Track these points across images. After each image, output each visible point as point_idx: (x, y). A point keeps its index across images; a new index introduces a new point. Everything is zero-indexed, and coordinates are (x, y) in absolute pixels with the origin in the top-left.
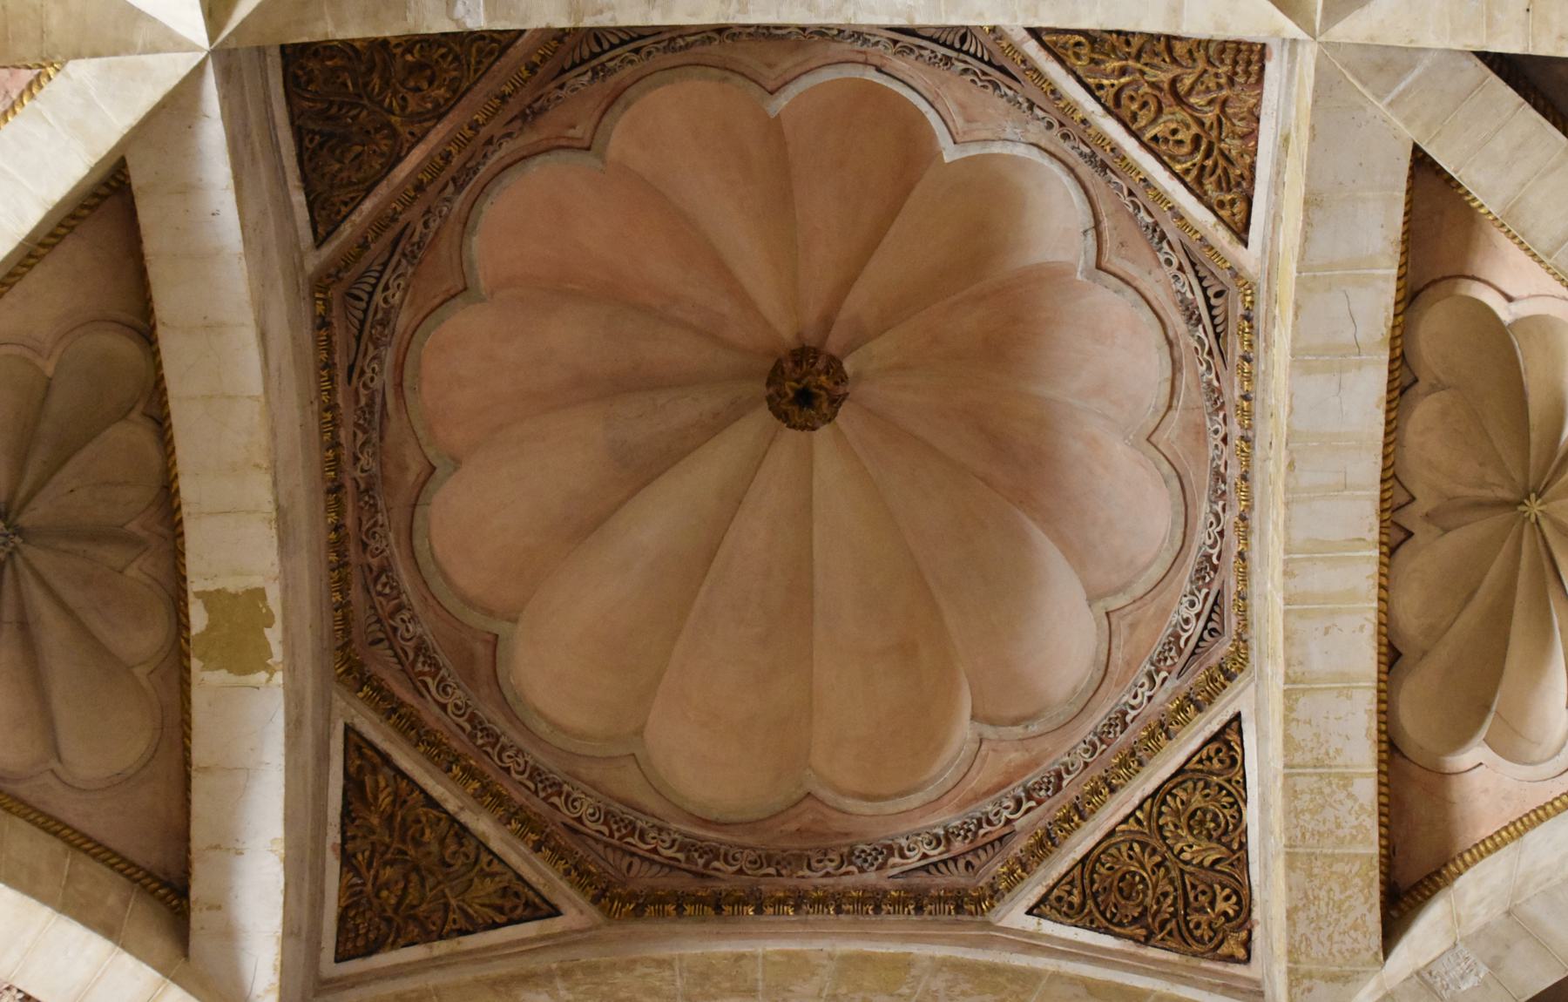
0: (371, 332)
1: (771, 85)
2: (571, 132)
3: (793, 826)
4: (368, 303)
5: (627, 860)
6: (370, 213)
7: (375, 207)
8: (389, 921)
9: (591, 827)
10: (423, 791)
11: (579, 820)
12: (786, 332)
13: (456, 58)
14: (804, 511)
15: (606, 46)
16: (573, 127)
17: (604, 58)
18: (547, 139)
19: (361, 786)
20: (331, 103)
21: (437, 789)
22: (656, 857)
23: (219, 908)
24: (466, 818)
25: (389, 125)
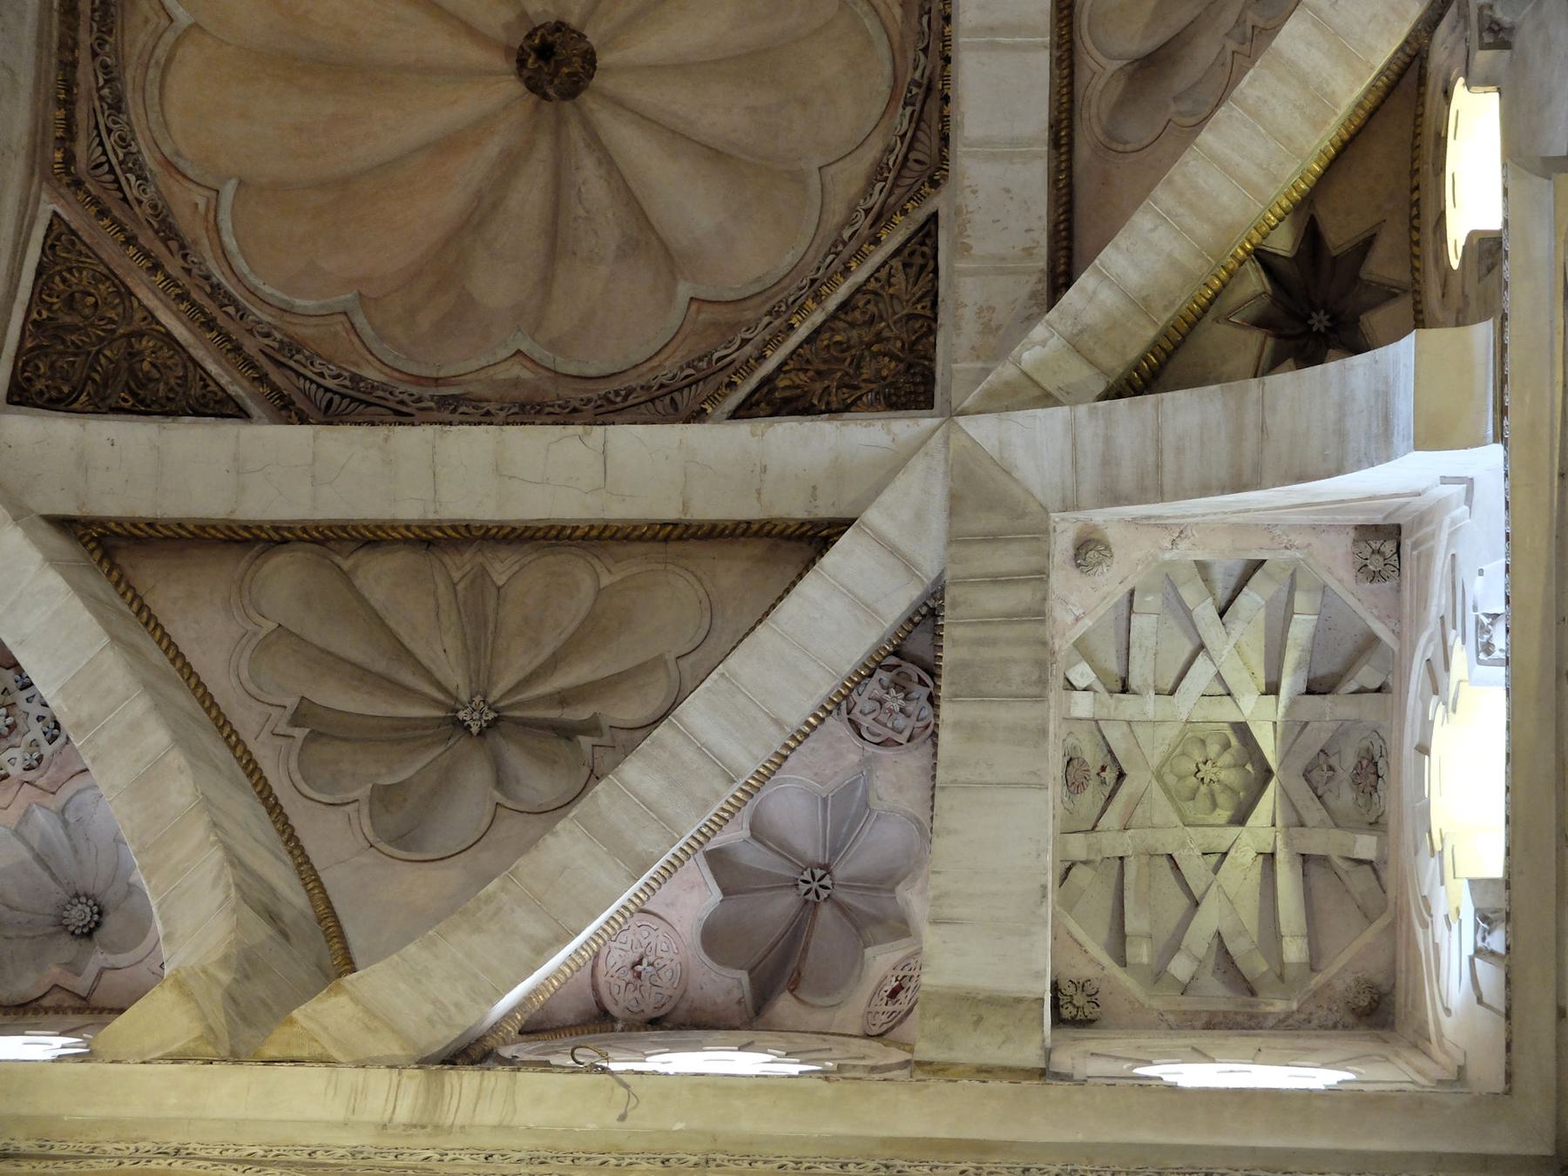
0: (364, 392)
1: (164, 22)
2: (202, 207)
3: (897, 11)
4: (335, 393)
5: (910, 164)
6: (221, 365)
7: (216, 361)
8: (910, 366)
9: (876, 199)
10: (800, 346)
11: (867, 211)
12: (512, 87)
13: (70, 270)
14: (681, 68)
15: (103, 159)
16: (197, 205)
17: (114, 161)
18: (207, 229)
19: (786, 401)
20: (89, 377)
21: (802, 332)
22: (909, 135)
23: (814, 488)
24: (832, 304)
25: (128, 336)
